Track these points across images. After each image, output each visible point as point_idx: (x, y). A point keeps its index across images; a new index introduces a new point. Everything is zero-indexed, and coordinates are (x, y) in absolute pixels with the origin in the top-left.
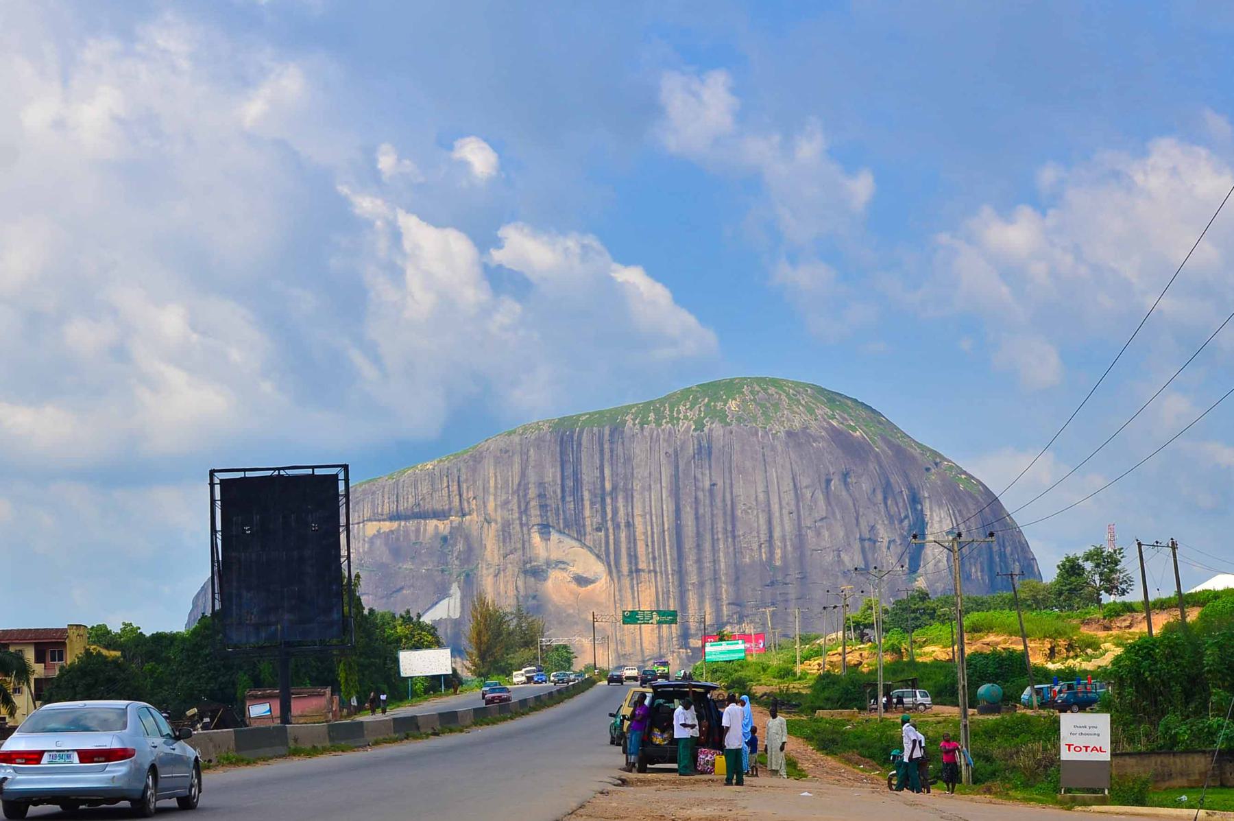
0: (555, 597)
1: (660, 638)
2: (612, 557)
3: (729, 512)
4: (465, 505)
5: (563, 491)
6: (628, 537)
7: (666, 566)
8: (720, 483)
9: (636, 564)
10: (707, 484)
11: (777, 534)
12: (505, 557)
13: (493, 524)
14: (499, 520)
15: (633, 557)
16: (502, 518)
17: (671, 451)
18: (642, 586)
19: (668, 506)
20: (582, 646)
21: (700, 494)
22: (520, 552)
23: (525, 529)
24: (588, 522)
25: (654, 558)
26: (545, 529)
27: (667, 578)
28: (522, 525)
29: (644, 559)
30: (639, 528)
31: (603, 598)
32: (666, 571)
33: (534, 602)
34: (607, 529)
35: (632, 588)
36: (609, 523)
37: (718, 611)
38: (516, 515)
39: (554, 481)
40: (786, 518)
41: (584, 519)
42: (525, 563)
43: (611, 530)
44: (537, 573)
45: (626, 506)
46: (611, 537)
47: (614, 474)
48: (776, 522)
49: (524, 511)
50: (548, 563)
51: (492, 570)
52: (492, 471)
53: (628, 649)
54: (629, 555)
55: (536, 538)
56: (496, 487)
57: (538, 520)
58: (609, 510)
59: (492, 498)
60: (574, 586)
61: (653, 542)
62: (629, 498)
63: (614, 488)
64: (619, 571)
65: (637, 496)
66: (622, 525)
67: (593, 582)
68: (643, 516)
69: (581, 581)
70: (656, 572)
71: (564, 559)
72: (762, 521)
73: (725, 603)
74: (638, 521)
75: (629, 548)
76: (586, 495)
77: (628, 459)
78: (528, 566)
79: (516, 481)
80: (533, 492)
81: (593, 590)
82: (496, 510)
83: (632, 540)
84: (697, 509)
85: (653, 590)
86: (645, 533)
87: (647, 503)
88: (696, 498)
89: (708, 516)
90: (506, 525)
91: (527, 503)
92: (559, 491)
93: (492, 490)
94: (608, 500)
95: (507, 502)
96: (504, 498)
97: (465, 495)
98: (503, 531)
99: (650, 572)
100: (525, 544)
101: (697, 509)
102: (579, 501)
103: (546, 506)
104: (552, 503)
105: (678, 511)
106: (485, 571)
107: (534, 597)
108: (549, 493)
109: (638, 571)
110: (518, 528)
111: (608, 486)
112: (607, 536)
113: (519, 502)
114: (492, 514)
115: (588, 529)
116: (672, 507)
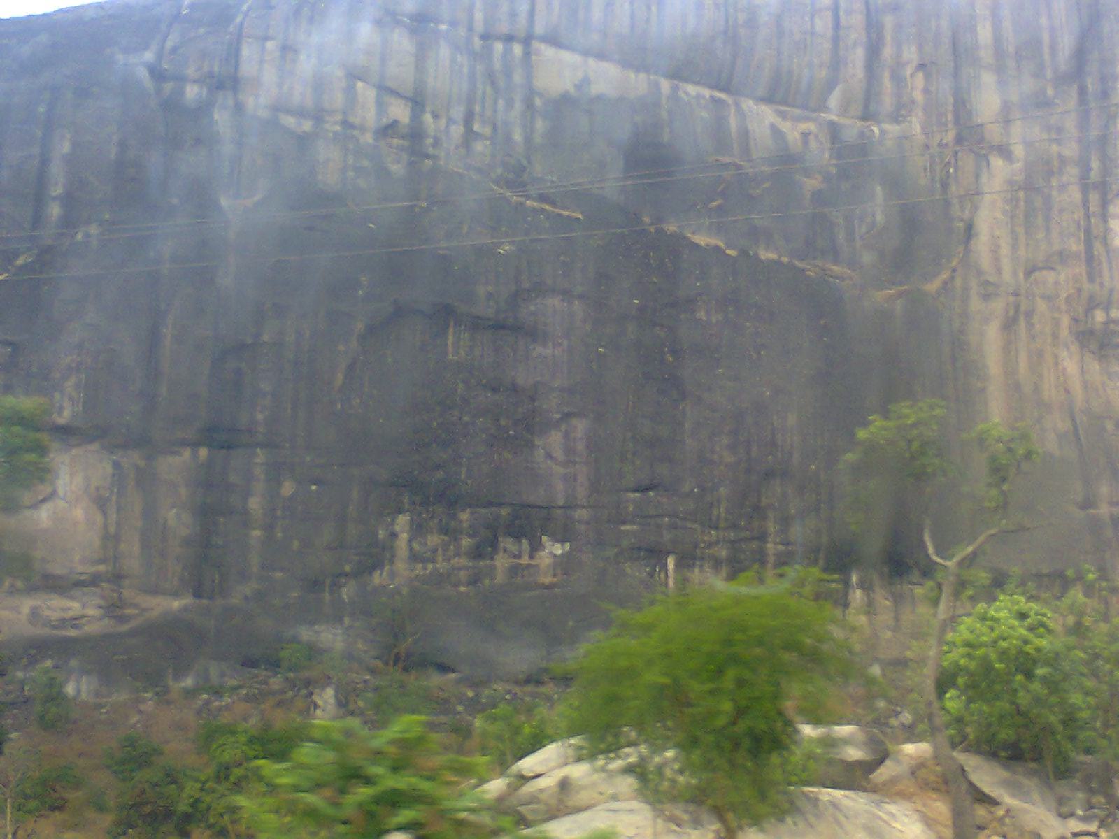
4: (887, 83)
12: (1028, 273)
14: (1019, 151)
16: (1028, 144)
22: (1080, 269)
38: (1071, 150)
42: (1092, 305)
51: (998, 305)
59: (988, 78)
78: (1099, 316)
93: (986, 55)
97: (888, 52)
106: (975, 304)
110: (1075, 194)
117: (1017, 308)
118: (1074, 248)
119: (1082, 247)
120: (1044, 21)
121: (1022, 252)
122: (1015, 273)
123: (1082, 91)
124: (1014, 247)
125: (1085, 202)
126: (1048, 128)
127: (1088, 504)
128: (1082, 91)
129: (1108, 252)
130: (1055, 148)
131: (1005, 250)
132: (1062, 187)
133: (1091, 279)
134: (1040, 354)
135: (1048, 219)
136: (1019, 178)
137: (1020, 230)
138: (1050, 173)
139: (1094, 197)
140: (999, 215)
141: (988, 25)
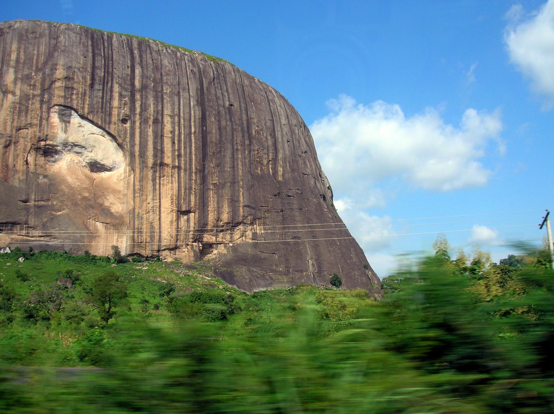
0: (70, 179)
1: (178, 229)
2: (137, 148)
3: (246, 129)
5: (93, 79)
6: (155, 133)
7: (191, 164)
8: (236, 105)
9: (162, 158)
10: (227, 104)
11: (280, 156)
13: (10, 96)
14: (18, 92)
15: (159, 152)
16: (21, 90)
17: (196, 70)
18: (165, 180)
19: (196, 113)
20: (97, 230)
21: (221, 109)
22: (37, 129)
23: (45, 107)
24: (115, 112)
25: (179, 156)
26: (66, 110)
27: (190, 175)
28: (42, 102)
29: (170, 155)
30: (168, 127)
31: (121, 186)
32: (191, 168)
33: (46, 180)
34: (134, 123)
35: (154, 180)
36: (138, 117)
37: (234, 211)
38: (38, 92)
39: (84, 69)
40: (286, 145)
41: (111, 108)
42: (40, 140)
43: (138, 124)
44: (49, 152)
45: (156, 105)
46: (137, 131)
47: (143, 76)
48: (280, 146)
49: (47, 89)
50: (65, 144)
52: (15, 46)
53: (145, 237)
54: (155, 148)
55: (55, 118)
56: (18, 61)
57: (62, 101)
58: (138, 105)
59: (12, 70)
60: (87, 171)
61: (179, 141)
62: (159, 98)
63: (144, 87)
64: (144, 162)
65: (166, 98)
66: (151, 122)
67: (110, 170)
68: (172, 117)
69: (96, 167)
70: (179, 168)
71: (83, 144)
72: (270, 143)
73: (241, 205)
74: (167, 121)
75: (155, 143)
76: (116, 88)
77: (157, 68)
79: (42, 59)
80: (60, 73)
81: (110, 178)
82: (15, 82)
83: (159, 137)
84: (219, 121)
85: (176, 185)
86: (173, 132)
87: (177, 106)
88: (219, 112)
89: (229, 129)
90: (26, 98)
91: (53, 82)
92: (89, 78)
93: (12, 63)
94: (138, 96)
95: (28, 77)
96: (26, 72)
98: (20, 103)
99: (173, 167)
100: (44, 119)
101: (219, 121)
102: (107, 91)
103: (73, 88)
104: (79, 88)
105: (203, 118)
107: (45, 177)
108: (78, 77)
109: (162, 165)
110: (38, 105)
111: (137, 84)
112: (133, 128)
113: (44, 80)
114: (11, 87)
115: (114, 119)
116: (198, 113)
117: (10, 141)
118: (36, 122)
119: (38, 122)
120: (36, 52)
121: (15, 124)
122: (12, 131)
123: (44, 74)
124: (12, 123)
125: (41, 108)
126: (30, 85)
127: (26, 201)
128: (44, 74)
129: (48, 123)
130: (32, 91)
131: (9, 123)
132: (33, 103)
133: (40, 132)
134: (18, 155)
135: (27, 113)
136: (18, 101)
137: (16, 117)
138: (29, 99)
139: (45, 107)
140: (8, 112)
141: (15, 53)
